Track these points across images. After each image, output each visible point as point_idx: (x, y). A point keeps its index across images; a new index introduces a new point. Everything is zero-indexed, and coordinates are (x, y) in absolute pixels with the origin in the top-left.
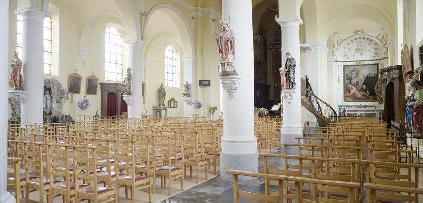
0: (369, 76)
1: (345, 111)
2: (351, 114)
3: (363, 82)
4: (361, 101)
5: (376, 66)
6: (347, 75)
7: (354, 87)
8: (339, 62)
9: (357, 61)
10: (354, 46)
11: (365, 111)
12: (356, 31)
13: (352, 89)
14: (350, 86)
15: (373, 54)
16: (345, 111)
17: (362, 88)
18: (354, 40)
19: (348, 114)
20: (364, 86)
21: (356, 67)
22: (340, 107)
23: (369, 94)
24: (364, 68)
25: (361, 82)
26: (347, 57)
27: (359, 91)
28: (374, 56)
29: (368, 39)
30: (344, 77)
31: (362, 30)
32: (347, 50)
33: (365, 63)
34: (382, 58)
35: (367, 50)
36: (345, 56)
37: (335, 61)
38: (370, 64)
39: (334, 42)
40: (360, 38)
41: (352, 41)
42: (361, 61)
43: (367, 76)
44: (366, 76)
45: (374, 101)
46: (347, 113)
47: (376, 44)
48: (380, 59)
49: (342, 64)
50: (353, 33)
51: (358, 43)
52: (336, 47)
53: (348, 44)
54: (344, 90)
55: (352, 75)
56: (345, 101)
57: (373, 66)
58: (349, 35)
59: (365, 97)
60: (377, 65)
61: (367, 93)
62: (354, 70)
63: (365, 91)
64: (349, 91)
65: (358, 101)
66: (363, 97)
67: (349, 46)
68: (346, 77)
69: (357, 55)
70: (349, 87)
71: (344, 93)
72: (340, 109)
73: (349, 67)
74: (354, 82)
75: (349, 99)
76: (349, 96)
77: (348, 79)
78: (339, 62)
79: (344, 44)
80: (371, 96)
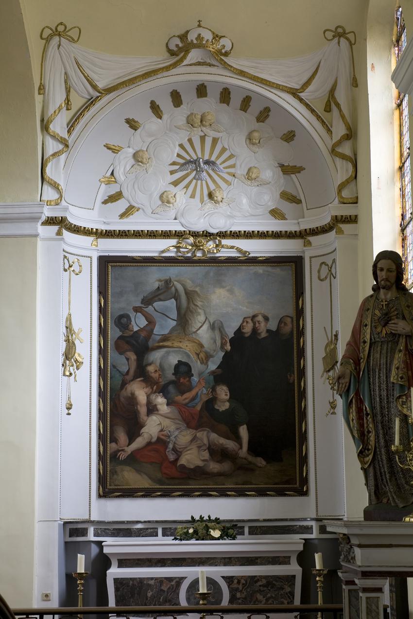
0: (248, 329)
1: (102, 562)
2: (140, 584)
3: (213, 366)
4: (205, 494)
5: (286, 273)
6: (122, 321)
7: (160, 401)
8: (76, 230)
9: (179, 235)
10: (167, 140)
11: (228, 560)
12: (183, 37)
13: (152, 409)
14: (140, 393)
15: (269, 199)
16: (102, 562)
17: (210, 403)
18: (165, 104)
19: (119, 583)
20: (223, 392)
21: (173, 271)
22: (73, 530)
23: (253, 449)
24: (219, 283)
25: (203, 370)
26: (121, 206)
27: (189, 426)
28: (276, 213)
29: (246, 103)
30: (103, 331)
31: (217, 37)
32: (123, 164)
33: (229, 249)
34: (327, 220)
35: (241, 171)
36: (115, 197)
37: (51, 221)
38: (254, 261)
39: (42, 89)
40: (201, 91)
41: (155, 109)
42: (207, 235)
43: (239, 332)
44: (231, 334)
45: (281, 493)
46: (114, 572)
47: (289, 137)
48: (314, 232)
49: (88, 250)
50: (167, 55)
51: (190, 122)
52: (59, 126)
53: (133, 124)
54: (102, 416)
55: (151, 322)
56: (109, 487)
57: (277, 271)
58: (139, 64)
59: (226, 466)
60: (296, 263)
61: (237, 438)
62: (165, 290)
63: (227, 424)
64: (134, 428)
65: (187, 494)
66: (214, 467)
67: (138, 141)
68: (114, 333)
69: (181, 197)
70: (133, 399)
71: (101, 438)
72: (70, 550)
73: (130, 270)
74: (162, 368)
75: (130, 477)
76: (133, 460)
77: (126, 345)
78: (76, 230)
79: (103, 122)
80: (260, 462)
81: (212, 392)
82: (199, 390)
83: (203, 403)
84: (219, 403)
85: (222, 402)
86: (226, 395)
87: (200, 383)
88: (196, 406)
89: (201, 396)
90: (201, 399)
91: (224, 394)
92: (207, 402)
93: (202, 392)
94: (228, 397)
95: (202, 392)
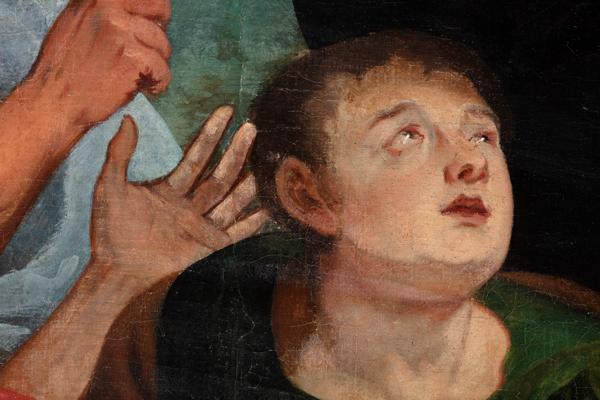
81: (258, 162)
82: (85, 125)
83: (124, 321)
84: (353, 321)
85: (407, 307)
86: (468, 209)
87: (103, 31)
88: (24, 345)
89: (98, 208)
90: (95, 269)
91: (436, 192)
92: (191, 292)
93: (117, 156)
94: (488, 242)
95: (117, 156)
